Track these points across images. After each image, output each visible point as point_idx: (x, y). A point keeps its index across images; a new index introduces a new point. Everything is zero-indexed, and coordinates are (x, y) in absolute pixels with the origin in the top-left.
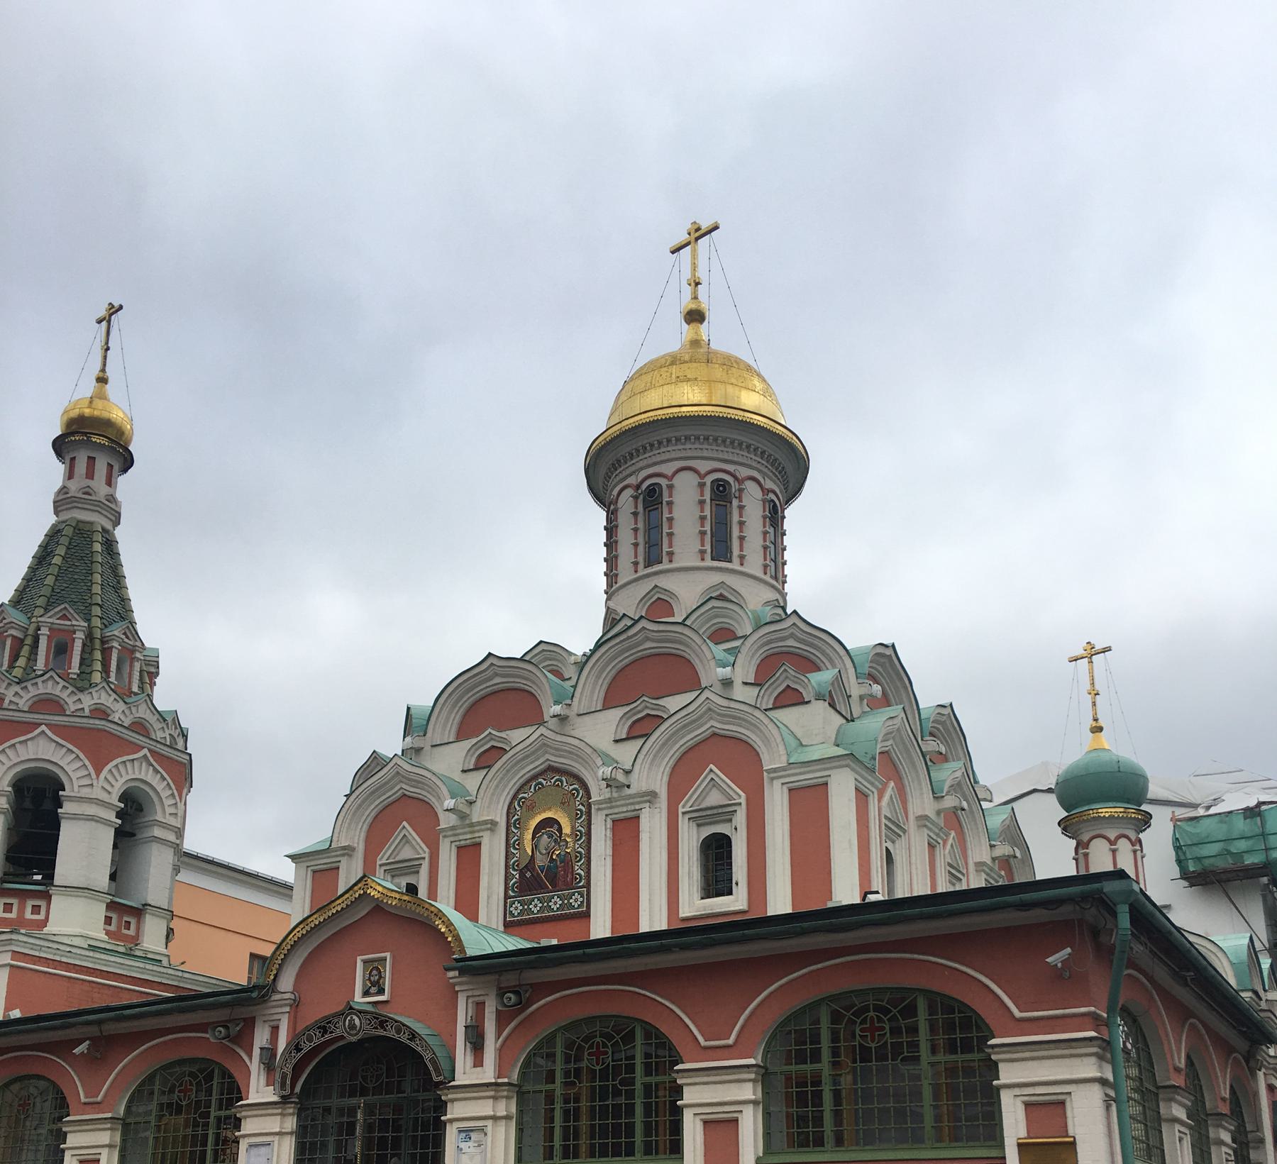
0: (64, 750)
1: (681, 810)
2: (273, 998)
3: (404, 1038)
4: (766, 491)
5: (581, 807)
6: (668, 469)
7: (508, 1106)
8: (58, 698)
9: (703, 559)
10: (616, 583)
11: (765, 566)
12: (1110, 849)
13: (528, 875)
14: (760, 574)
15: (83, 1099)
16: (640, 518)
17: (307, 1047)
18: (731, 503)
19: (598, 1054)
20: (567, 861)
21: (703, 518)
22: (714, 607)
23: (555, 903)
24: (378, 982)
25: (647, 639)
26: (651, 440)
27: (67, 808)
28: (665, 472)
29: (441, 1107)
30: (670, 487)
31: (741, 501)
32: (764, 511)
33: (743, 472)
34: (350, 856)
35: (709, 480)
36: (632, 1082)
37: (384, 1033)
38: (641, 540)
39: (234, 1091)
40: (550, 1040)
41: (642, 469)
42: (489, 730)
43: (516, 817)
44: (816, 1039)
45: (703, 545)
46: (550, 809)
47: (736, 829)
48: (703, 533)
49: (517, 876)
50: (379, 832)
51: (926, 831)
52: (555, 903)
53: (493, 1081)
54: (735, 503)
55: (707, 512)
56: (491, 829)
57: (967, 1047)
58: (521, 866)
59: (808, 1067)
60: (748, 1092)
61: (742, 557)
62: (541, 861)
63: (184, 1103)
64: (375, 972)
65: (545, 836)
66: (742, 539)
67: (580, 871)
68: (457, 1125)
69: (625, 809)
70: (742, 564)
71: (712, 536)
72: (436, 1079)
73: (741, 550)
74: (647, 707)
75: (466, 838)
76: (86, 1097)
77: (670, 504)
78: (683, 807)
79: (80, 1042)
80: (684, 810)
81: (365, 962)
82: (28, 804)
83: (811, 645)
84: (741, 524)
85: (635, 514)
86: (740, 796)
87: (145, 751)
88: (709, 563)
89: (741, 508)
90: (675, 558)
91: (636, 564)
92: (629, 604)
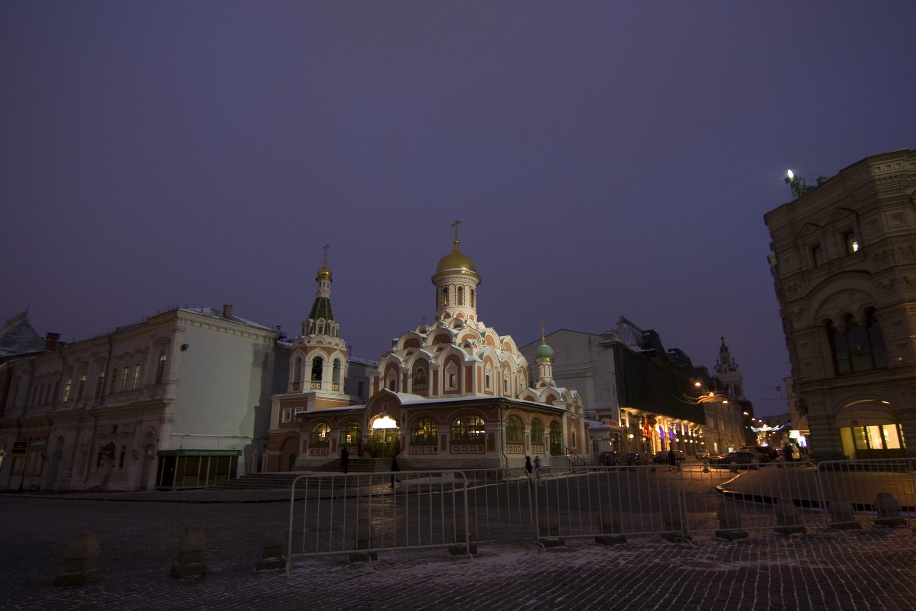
1: (446, 368)
4: (470, 287)
35: (457, 287)
62: (419, 377)
75: (405, 373)
79: (331, 417)
82: (316, 363)
88: (457, 305)
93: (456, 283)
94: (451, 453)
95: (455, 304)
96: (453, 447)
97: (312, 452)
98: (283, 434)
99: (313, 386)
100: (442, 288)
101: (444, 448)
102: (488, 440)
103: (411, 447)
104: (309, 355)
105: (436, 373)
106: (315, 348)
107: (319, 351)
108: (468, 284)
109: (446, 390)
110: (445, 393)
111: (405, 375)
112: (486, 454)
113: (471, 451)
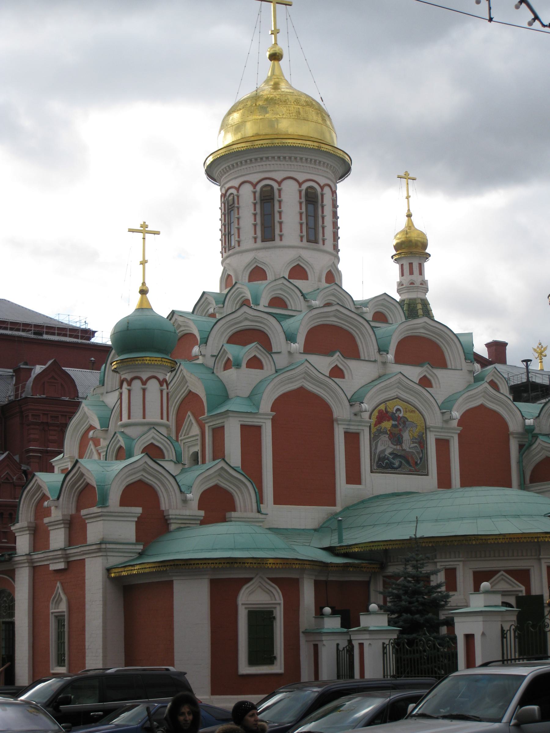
4: (300, 184)
6: (236, 183)
11: (302, 237)
14: (301, 244)
22: (238, 288)
30: (238, 197)
32: (300, 198)
45: (255, 234)
61: (281, 236)
70: (281, 240)
73: (281, 231)
77: (238, 208)
78: (181, 436)
80: (183, 437)
84: (280, 213)
88: (259, 244)
95: (255, 242)
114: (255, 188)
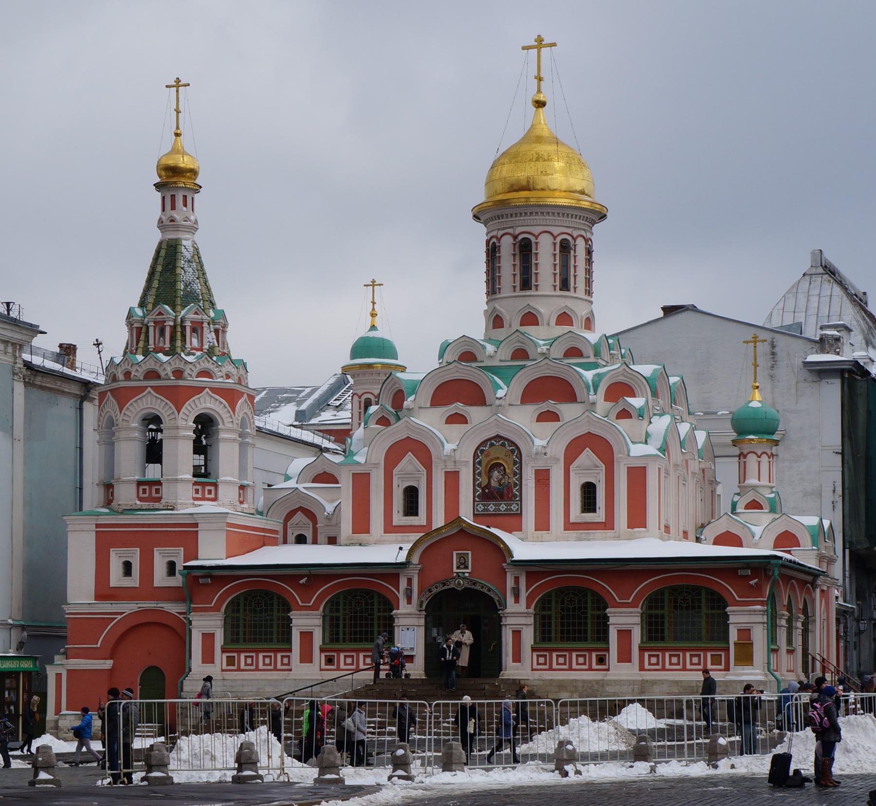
0: (218, 402)
2: (411, 566)
3: (485, 591)
5: (516, 459)
6: (536, 230)
7: (531, 620)
8: (209, 371)
9: (555, 290)
10: (500, 292)
12: (757, 460)
13: (487, 491)
15: (300, 604)
16: (517, 258)
17: (435, 591)
18: (570, 253)
19: (571, 601)
20: (509, 488)
21: (555, 265)
23: (503, 507)
24: (464, 563)
25: (548, 369)
26: (526, 211)
27: (222, 435)
28: (534, 233)
29: (500, 619)
30: (537, 243)
31: (575, 252)
33: (575, 234)
34: (377, 468)
36: (586, 613)
37: (476, 588)
38: (518, 272)
39: (389, 605)
40: (549, 595)
41: (518, 226)
42: (455, 404)
43: (479, 459)
44: (663, 601)
45: (555, 282)
46: (498, 458)
47: (599, 481)
48: (555, 274)
49: (480, 491)
50: (394, 455)
51: (678, 471)
52: (503, 507)
53: (526, 611)
54: (572, 252)
55: (558, 262)
56: (465, 465)
57: (719, 608)
58: (483, 486)
59: (659, 612)
60: (638, 620)
61: (575, 288)
62: (494, 484)
63: (358, 609)
64: (462, 559)
65: (496, 472)
66: (575, 276)
67: (516, 492)
68: (508, 627)
69: (542, 465)
70: (575, 291)
71: (560, 275)
72: (499, 608)
74: (548, 407)
75: (451, 468)
76: (302, 602)
77: (536, 254)
79: (302, 577)
81: (457, 554)
83: (631, 379)
85: (514, 255)
86: (602, 467)
87: (245, 396)
89: (575, 257)
90: (539, 288)
91: (515, 287)
92: (510, 311)
93: (556, 231)
94: (642, 668)
95: (555, 290)
96: (646, 654)
97: (230, 661)
98: (119, 617)
99: (197, 491)
100: (515, 237)
101: (625, 657)
102: (735, 644)
103: (535, 654)
104: (182, 410)
105: (543, 478)
106: (200, 390)
107: (208, 398)
108: (583, 233)
109: (573, 519)
110: (569, 526)
111: (452, 478)
112: (731, 671)
113: (692, 664)
114: (555, 239)
